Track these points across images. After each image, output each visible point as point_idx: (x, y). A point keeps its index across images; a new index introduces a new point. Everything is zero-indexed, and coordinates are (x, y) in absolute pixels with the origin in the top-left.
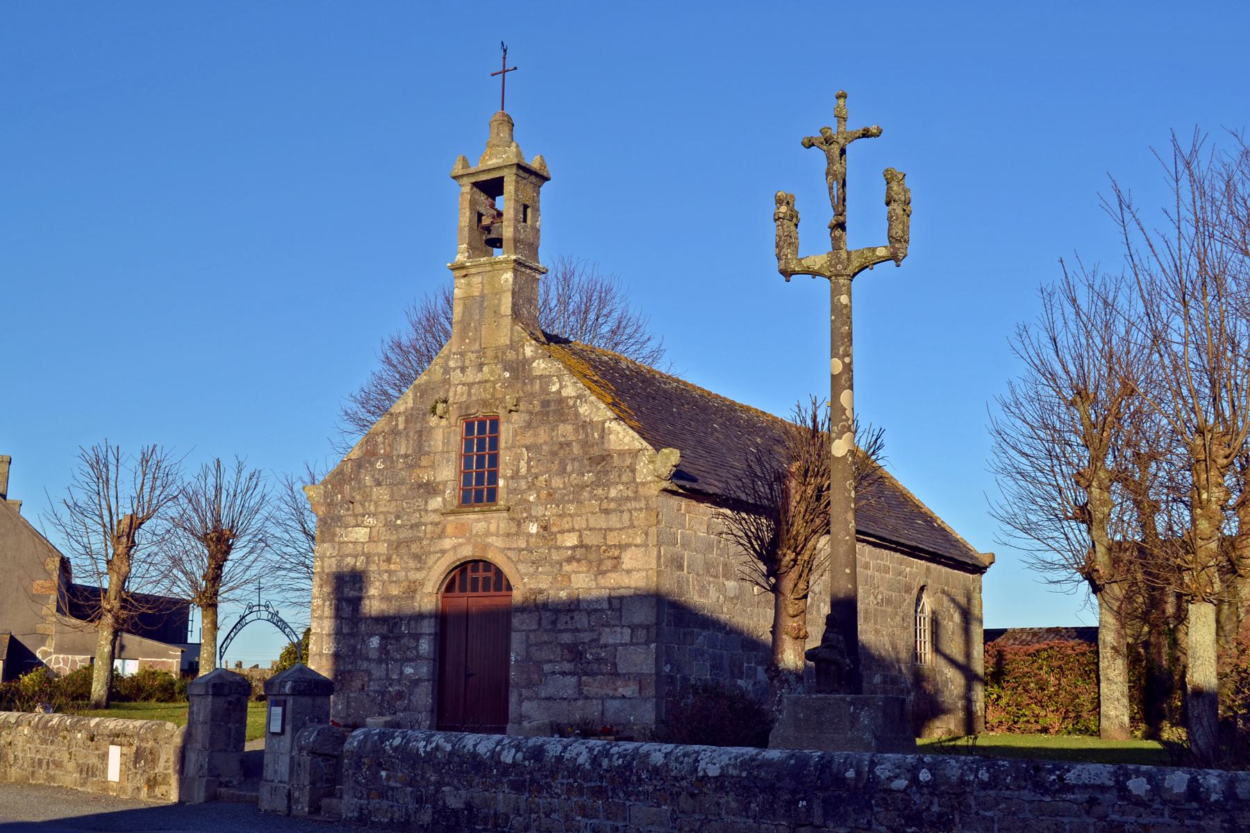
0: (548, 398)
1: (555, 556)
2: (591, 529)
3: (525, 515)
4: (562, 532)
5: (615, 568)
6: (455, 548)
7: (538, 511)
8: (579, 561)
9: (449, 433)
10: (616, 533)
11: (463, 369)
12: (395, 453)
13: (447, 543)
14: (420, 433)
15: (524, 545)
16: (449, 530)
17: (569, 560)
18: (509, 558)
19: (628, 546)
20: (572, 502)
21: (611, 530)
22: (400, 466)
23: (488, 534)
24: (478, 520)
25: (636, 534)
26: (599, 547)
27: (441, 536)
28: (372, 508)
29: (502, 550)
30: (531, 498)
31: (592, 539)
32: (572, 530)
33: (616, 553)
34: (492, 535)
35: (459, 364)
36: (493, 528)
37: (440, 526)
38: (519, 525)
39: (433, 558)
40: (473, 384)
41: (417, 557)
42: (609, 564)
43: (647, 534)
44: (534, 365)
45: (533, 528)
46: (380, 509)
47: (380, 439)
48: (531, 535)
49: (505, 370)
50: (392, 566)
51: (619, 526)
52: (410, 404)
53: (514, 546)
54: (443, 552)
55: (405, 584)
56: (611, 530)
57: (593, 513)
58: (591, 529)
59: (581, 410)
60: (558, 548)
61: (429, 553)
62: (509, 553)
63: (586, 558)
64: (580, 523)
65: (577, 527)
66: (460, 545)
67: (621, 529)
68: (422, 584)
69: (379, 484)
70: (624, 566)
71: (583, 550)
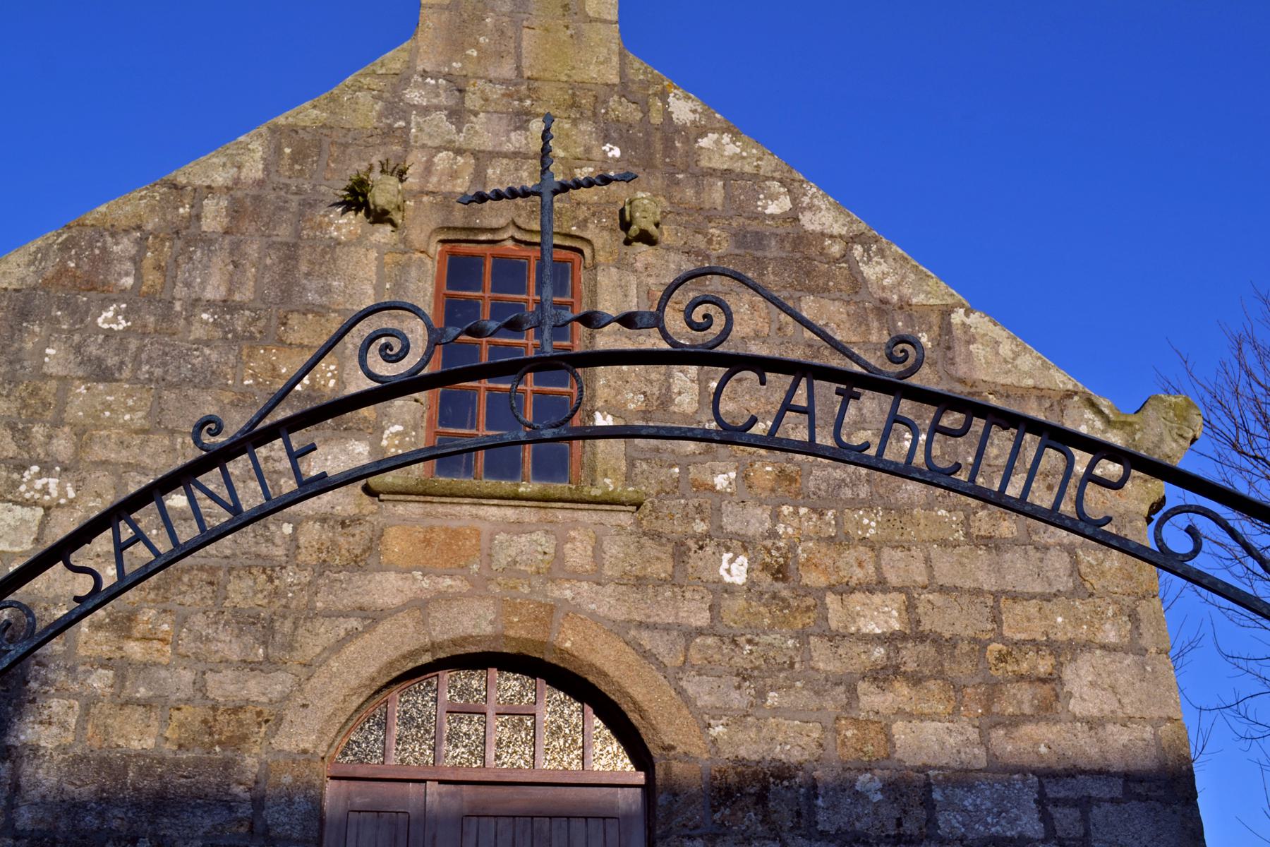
0: (754, 226)
1: (824, 659)
2: (942, 589)
3: (700, 527)
4: (844, 590)
5: (1046, 711)
6: (420, 606)
7: (756, 520)
8: (916, 680)
9: (404, 268)
10: (1032, 607)
11: (457, 115)
12: (180, 291)
13: (387, 588)
14: (290, 252)
15: (702, 619)
16: (396, 544)
17: (882, 676)
18: (647, 655)
19: (1088, 646)
20: (869, 506)
21: (1015, 597)
22: (198, 332)
23: (556, 569)
24: (519, 527)
25: (1100, 615)
26: (980, 645)
27: (365, 559)
28: (62, 446)
29: (619, 629)
30: (720, 481)
31: (944, 618)
32: (881, 585)
33: (1044, 666)
34: (575, 576)
35: (451, 103)
36: (578, 554)
37: (361, 534)
38: (680, 552)
39: (326, 633)
40: (495, 155)
41: (256, 624)
42: (1022, 698)
43: (1134, 617)
44: (704, 142)
45: (736, 571)
46: (98, 453)
47: (124, 246)
48: (730, 589)
49: (606, 139)
50: (135, 649)
51: (1038, 588)
52: (254, 169)
53: (667, 617)
54: (372, 617)
55: (192, 715)
56: (1015, 597)
57: (944, 543)
58: (942, 589)
59: (871, 272)
60: (834, 637)
61: (311, 615)
62: (646, 638)
63: (940, 675)
64: (902, 567)
65: (893, 579)
66: (444, 597)
67: (1047, 598)
68: (272, 720)
69: (102, 374)
70: (1075, 706)
71: (928, 649)
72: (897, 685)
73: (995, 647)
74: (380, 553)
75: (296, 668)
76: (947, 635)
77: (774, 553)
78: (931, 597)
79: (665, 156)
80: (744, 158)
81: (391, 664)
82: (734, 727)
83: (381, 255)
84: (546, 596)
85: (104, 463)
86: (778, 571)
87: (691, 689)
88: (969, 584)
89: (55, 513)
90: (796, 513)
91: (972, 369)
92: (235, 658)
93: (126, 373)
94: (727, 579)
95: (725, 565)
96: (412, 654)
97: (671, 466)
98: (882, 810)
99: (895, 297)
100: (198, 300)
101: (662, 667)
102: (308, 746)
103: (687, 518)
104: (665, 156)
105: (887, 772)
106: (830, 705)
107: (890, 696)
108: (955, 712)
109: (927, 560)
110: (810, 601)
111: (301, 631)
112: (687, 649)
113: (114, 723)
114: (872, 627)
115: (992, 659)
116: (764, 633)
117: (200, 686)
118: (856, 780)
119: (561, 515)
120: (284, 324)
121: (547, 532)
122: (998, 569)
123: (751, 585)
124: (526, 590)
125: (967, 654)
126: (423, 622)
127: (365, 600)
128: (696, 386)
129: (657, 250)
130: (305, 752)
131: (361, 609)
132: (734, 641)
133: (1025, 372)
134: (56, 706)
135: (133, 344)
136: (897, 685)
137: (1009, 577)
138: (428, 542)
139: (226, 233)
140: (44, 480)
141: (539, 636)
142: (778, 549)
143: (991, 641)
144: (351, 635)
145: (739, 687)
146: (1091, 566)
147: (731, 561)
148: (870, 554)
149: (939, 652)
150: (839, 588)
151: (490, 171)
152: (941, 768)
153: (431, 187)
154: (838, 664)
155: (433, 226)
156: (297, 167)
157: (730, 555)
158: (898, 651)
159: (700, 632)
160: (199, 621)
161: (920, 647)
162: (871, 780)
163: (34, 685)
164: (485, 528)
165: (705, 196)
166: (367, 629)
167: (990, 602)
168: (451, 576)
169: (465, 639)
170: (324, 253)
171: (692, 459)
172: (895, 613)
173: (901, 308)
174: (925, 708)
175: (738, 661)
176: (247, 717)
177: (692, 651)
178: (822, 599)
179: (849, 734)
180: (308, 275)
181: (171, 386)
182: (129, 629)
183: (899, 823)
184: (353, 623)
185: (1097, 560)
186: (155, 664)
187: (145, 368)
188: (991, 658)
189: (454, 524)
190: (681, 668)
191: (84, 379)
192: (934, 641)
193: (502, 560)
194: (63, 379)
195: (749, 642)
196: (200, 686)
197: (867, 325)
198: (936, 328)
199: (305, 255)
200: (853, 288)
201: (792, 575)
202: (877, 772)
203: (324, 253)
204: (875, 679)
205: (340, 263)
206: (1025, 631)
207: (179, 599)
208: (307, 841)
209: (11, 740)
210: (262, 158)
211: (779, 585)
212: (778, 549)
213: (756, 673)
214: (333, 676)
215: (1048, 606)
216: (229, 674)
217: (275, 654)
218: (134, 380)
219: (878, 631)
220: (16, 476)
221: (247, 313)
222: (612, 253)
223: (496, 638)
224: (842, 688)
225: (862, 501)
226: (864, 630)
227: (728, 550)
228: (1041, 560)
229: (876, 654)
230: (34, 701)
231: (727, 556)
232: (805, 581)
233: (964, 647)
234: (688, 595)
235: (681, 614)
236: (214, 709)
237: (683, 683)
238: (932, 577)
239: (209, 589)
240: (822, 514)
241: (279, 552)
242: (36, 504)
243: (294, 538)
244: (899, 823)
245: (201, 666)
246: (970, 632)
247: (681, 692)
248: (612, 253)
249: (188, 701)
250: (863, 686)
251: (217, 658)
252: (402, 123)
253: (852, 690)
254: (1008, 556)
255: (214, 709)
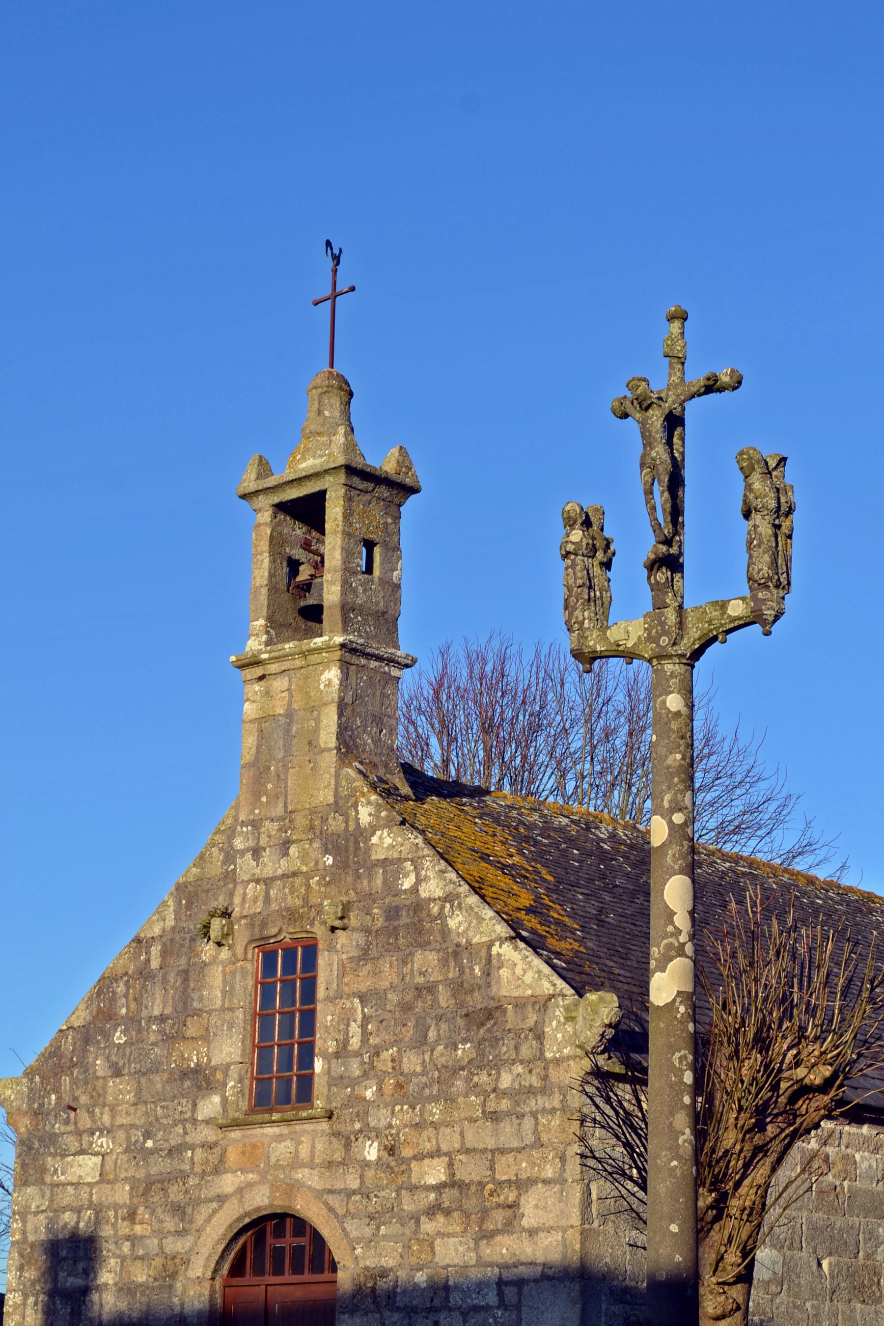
0: (396, 901)
1: (408, 1205)
2: (468, 1151)
3: (358, 1126)
4: (419, 1157)
5: (509, 1227)
6: (240, 1191)
7: (379, 1118)
8: (447, 1213)
9: (233, 973)
10: (510, 1158)
11: (256, 852)
12: (145, 1013)
13: (228, 1182)
14: (185, 974)
15: (355, 1185)
16: (232, 1156)
17: (432, 1211)
18: (331, 1209)
19: (532, 1182)
20: (435, 1099)
21: (502, 1151)
22: (152, 1038)
23: (295, 1163)
24: (280, 1138)
25: (544, 1159)
26: (481, 1185)
27: (218, 1169)
28: (106, 1119)
29: (320, 1194)
30: (369, 1094)
31: (471, 1170)
32: (436, 1153)
33: (512, 1197)
34: (303, 1165)
35: (251, 843)
36: (304, 1152)
37: (217, 1150)
38: (347, 1145)
39: (204, 1211)
40: (274, 879)
41: (178, 1210)
42: (499, 1217)
43: (563, 1159)
44: (375, 840)
45: (372, 1152)
46: (120, 1120)
47: (121, 988)
48: (367, 1164)
49: (326, 851)
50: (138, 1229)
51: (515, 1144)
52: (170, 922)
53: (339, 1185)
54: (221, 1199)
55: (158, 1262)
56: (502, 1151)
57: (472, 1120)
58: (468, 1151)
59: (452, 923)
60: (413, 1189)
61: (199, 1202)
62: (332, 1200)
63: (460, 1208)
64: (449, 1140)
65: (444, 1148)
66: (250, 1185)
67: (519, 1150)
68: (186, 1262)
69: (117, 1073)
70: (525, 1222)
71: (455, 1192)
72: (438, 1216)
73: (490, 1186)
74: (225, 1163)
75: (194, 1233)
76: (467, 1182)
77: (389, 1138)
78: (461, 1157)
79: (355, 856)
80: (394, 846)
81: (230, 1226)
82: (365, 1248)
83: (224, 967)
84: (291, 1179)
85: (122, 1125)
86: (391, 1150)
87: (348, 1227)
88: (482, 1146)
89: (106, 1157)
90: (402, 1109)
91: (499, 989)
92: (173, 1230)
93: (126, 1071)
94: (368, 1158)
95: (367, 1149)
96: (238, 1220)
97: (347, 1087)
98: (425, 1293)
99: (464, 940)
100: (151, 1017)
101: (336, 1216)
102: (199, 1274)
103: (352, 1121)
104: (355, 856)
105: (429, 1270)
106: (407, 1232)
107: (434, 1224)
108: (465, 1231)
109: (462, 1133)
110: (404, 1167)
111: (195, 1212)
112: (347, 1204)
113: (132, 1269)
114: (432, 1181)
115: (487, 1196)
116: (383, 1190)
117: (161, 1247)
118: (415, 1275)
119: (297, 1127)
120: (185, 1025)
121: (292, 1139)
122: (496, 1133)
123: (379, 1158)
124: (282, 1176)
125: (474, 1193)
126: (241, 1201)
127: (219, 1191)
128: (360, 1030)
129: (348, 932)
130: (198, 1278)
131: (218, 1196)
132: (368, 1197)
133: (528, 985)
134: (112, 1262)
135: (128, 1050)
136: (438, 1216)
137: (502, 1139)
138: (243, 1153)
139: (161, 968)
140: (101, 1140)
141: (287, 1204)
142: (391, 1135)
143: (488, 1183)
144: (215, 1212)
145: (368, 1225)
146: (544, 1125)
147: (371, 1146)
148: (435, 1132)
149: (461, 1194)
150: (419, 1156)
151: (272, 893)
152: (455, 1266)
153: (245, 913)
154: (413, 1206)
155: (246, 940)
156: (188, 913)
157: (370, 1142)
158: (441, 1194)
159: (354, 1192)
160: (159, 1211)
161: (452, 1191)
162: (422, 1275)
163: (104, 1252)
164: (266, 1140)
165: (373, 883)
166: (221, 1207)
167: (490, 1157)
168: (252, 1172)
169: (259, 1209)
170: (199, 973)
171: (357, 1081)
172: (443, 1170)
173: (466, 948)
174: (450, 1229)
175: (371, 1209)
176: (177, 1261)
177: (350, 1205)
178: (409, 1165)
179: (415, 1248)
180: (193, 989)
181: (144, 1074)
182: (135, 1219)
183: (432, 1301)
184: (215, 1205)
185: (547, 1120)
186: (145, 1236)
187: (133, 1065)
188: (486, 1193)
189: (254, 1140)
190: (345, 1216)
191: (112, 1077)
192: (459, 1186)
193: (273, 1160)
194: (104, 1078)
195: (376, 1196)
196: (161, 1247)
197: (448, 966)
198: (484, 960)
199: (192, 975)
200: (443, 938)
201: (397, 1153)
202: (425, 1270)
203: (199, 973)
204: (428, 1214)
205: (207, 978)
206: (506, 1173)
207: (151, 1199)
208: (201, 1324)
209: (98, 1282)
210: (174, 911)
211: (391, 1158)
212: (391, 1135)
213: (377, 1215)
214: (208, 1236)
215: (519, 1156)
216: (170, 1239)
217: (187, 1226)
218: (130, 1074)
219: (434, 1183)
220: (91, 1139)
221: (170, 1021)
222: (325, 940)
223: (271, 1205)
224: (413, 1221)
225: (434, 1097)
226: (428, 1183)
227: (369, 1139)
228: (520, 1124)
229: (431, 1198)
230: (105, 1261)
231: (368, 1143)
232: (403, 1154)
233: (473, 1188)
234: (350, 1170)
235: (348, 1182)
236: (166, 1258)
237: (345, 1225)
238: (463, 1143)
239: (161, 1193)
240: (414, 1109)
241: (187, 1167)
242: (99, 1154)
243: (192, 1159)
244: (432, 1301)
245: (161, 1236)
246: (478, 1178)
247: (344, 1230)
248: (325, 940)
249: (157, 1255)
250: (423, 1218)
251: (165, 1231)
252: (232, 867)
253: (418, 1221)
254: (502, 1125)
255: (166, 1258)
